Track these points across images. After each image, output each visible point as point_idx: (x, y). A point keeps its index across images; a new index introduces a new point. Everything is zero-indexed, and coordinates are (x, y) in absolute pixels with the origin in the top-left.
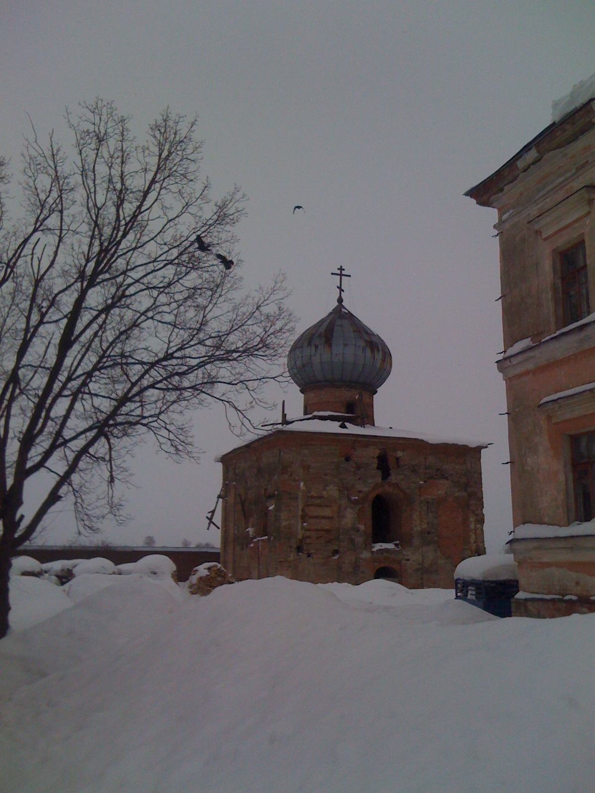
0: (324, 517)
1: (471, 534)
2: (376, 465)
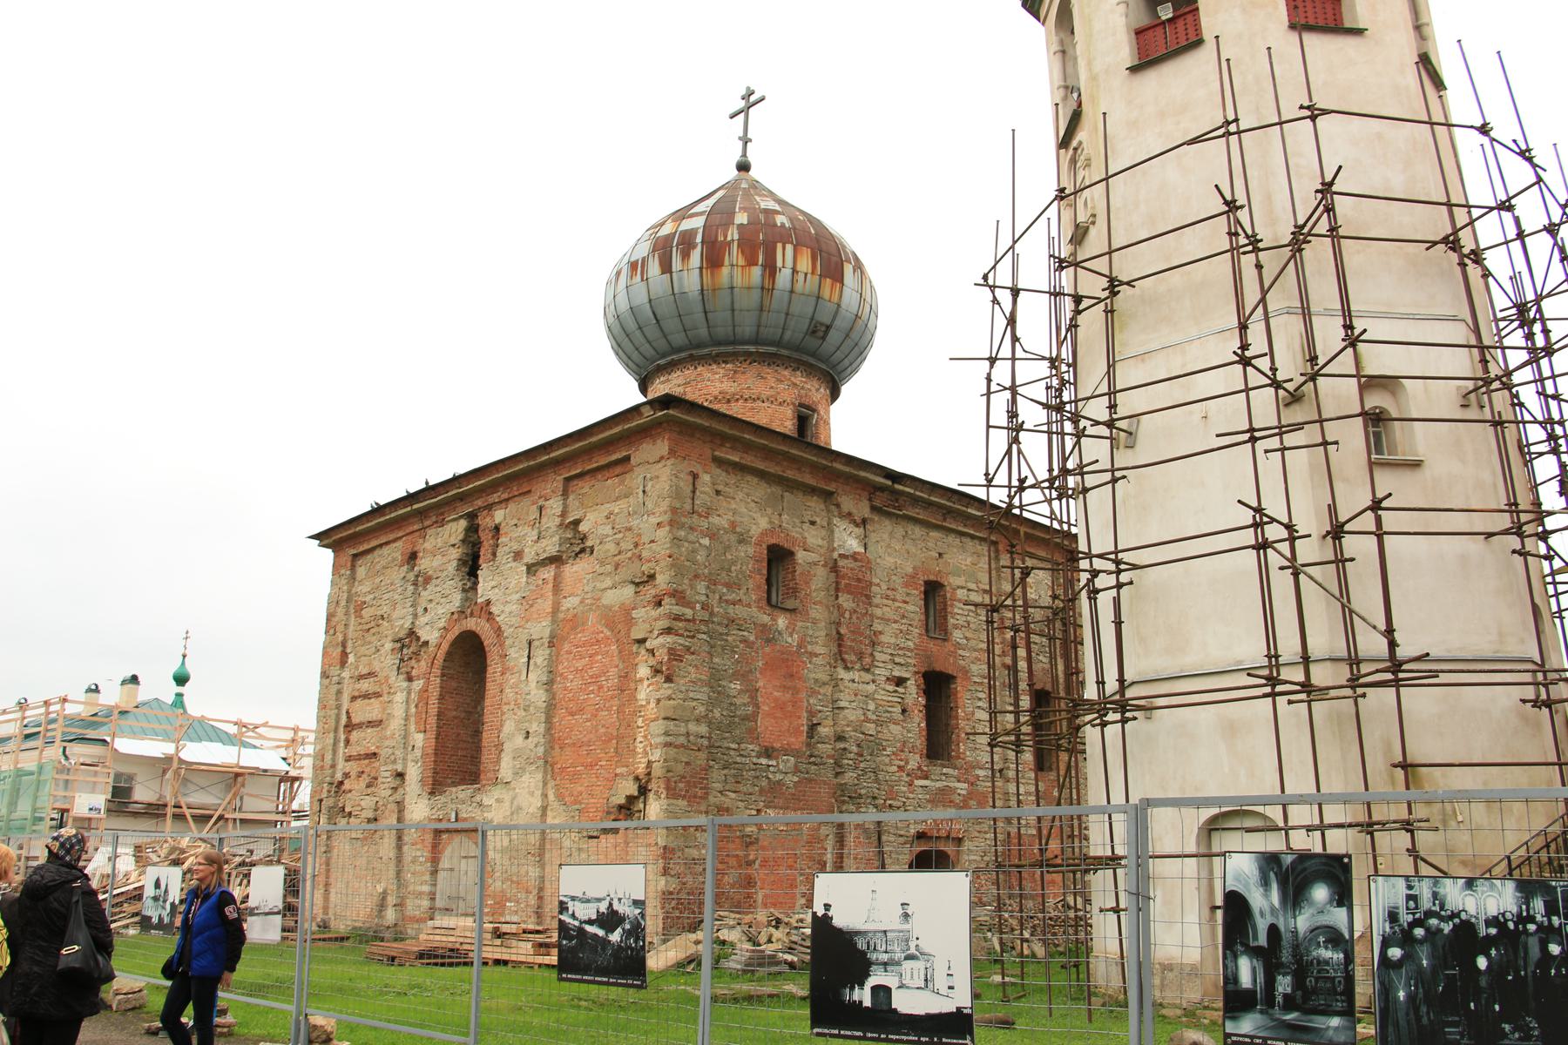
0: (370, 724)
1: (640, 723)
2: (455, 563)
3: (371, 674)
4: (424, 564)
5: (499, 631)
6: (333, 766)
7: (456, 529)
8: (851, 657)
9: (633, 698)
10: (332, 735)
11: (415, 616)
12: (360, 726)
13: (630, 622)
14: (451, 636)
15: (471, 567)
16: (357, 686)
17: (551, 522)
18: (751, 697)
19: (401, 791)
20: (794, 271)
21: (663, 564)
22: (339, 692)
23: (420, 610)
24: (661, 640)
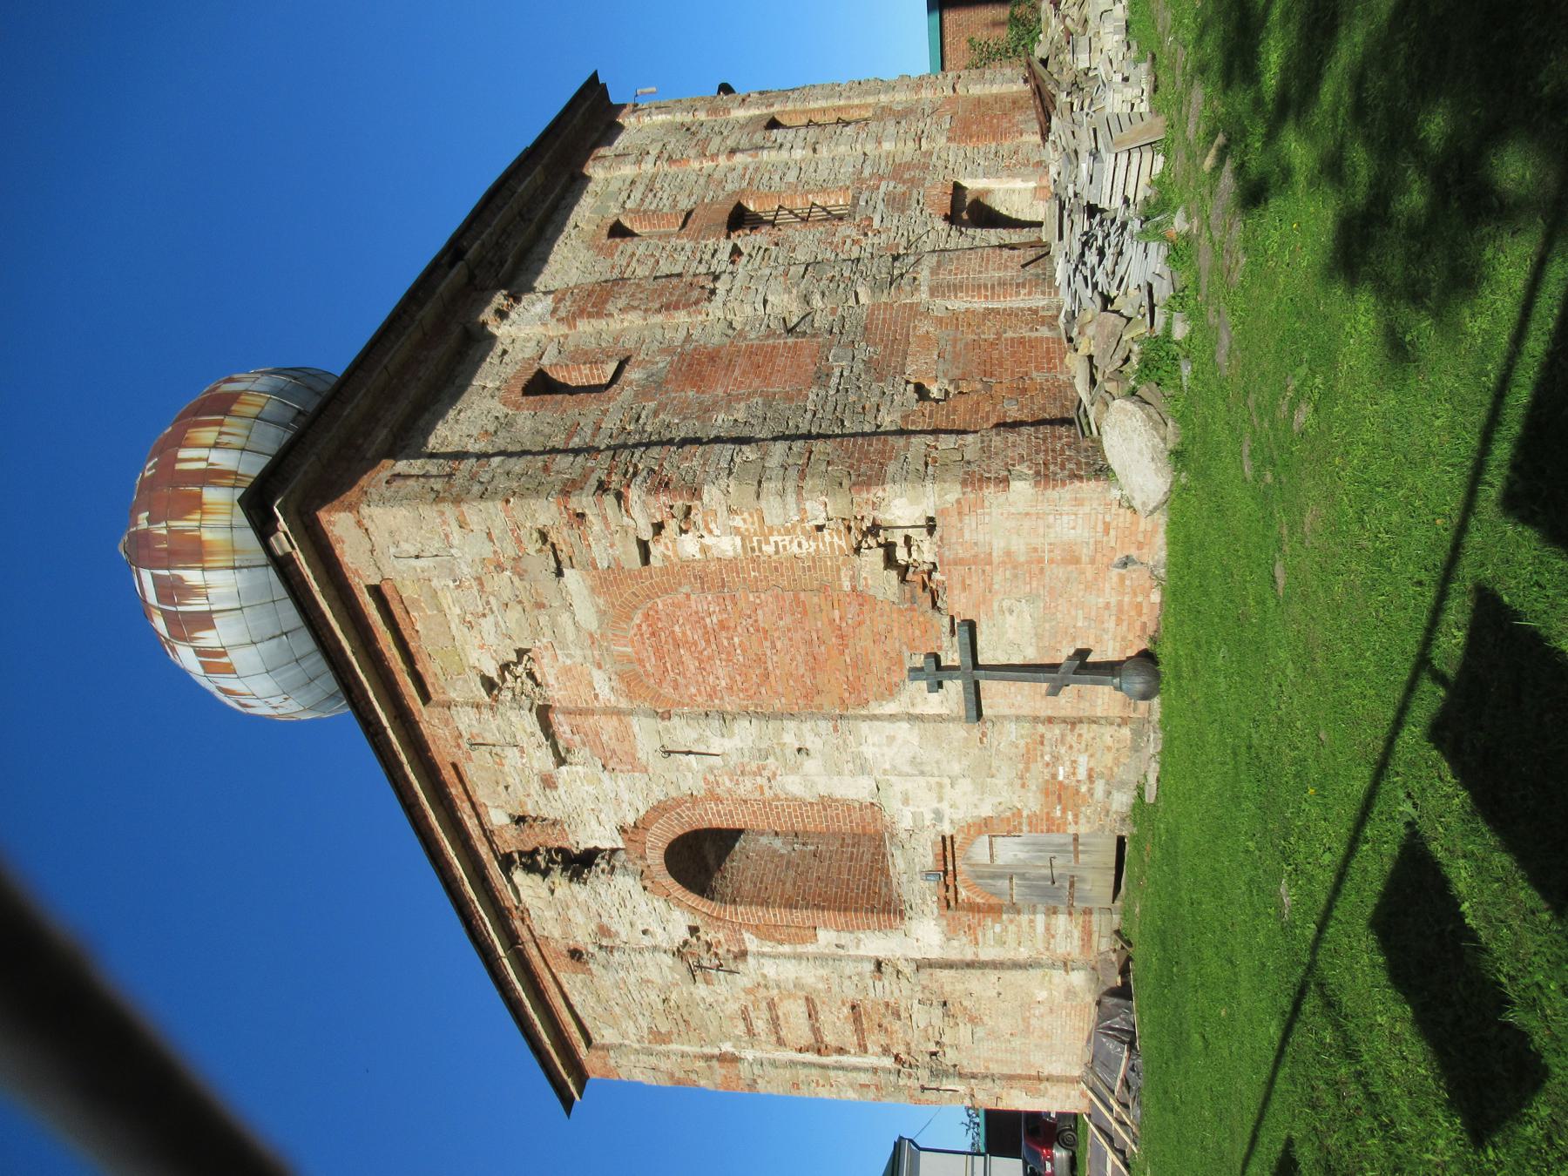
0: (812, 1014)
1: (769, 549)
2: (575, 887)
3: (745, 1015)
4: (583, 937)
5: (659, 810)
6: (875, 1070)
7: (529, 890)
8: (696, 294)
9: (731, 565)
10: (832, 1073)
11: (655, 948)
12: (816, 1031)
13: (616, 568)
14: (678, 890)
15: (579, 863)
16: (763, 1038)
17: (491, 727)
18: (738, 400)
19: (902, 966)
20: (216, 446)
21: (519, 516)
22: (773, 1063)
23: (646, 941)
24: (636, 510)
